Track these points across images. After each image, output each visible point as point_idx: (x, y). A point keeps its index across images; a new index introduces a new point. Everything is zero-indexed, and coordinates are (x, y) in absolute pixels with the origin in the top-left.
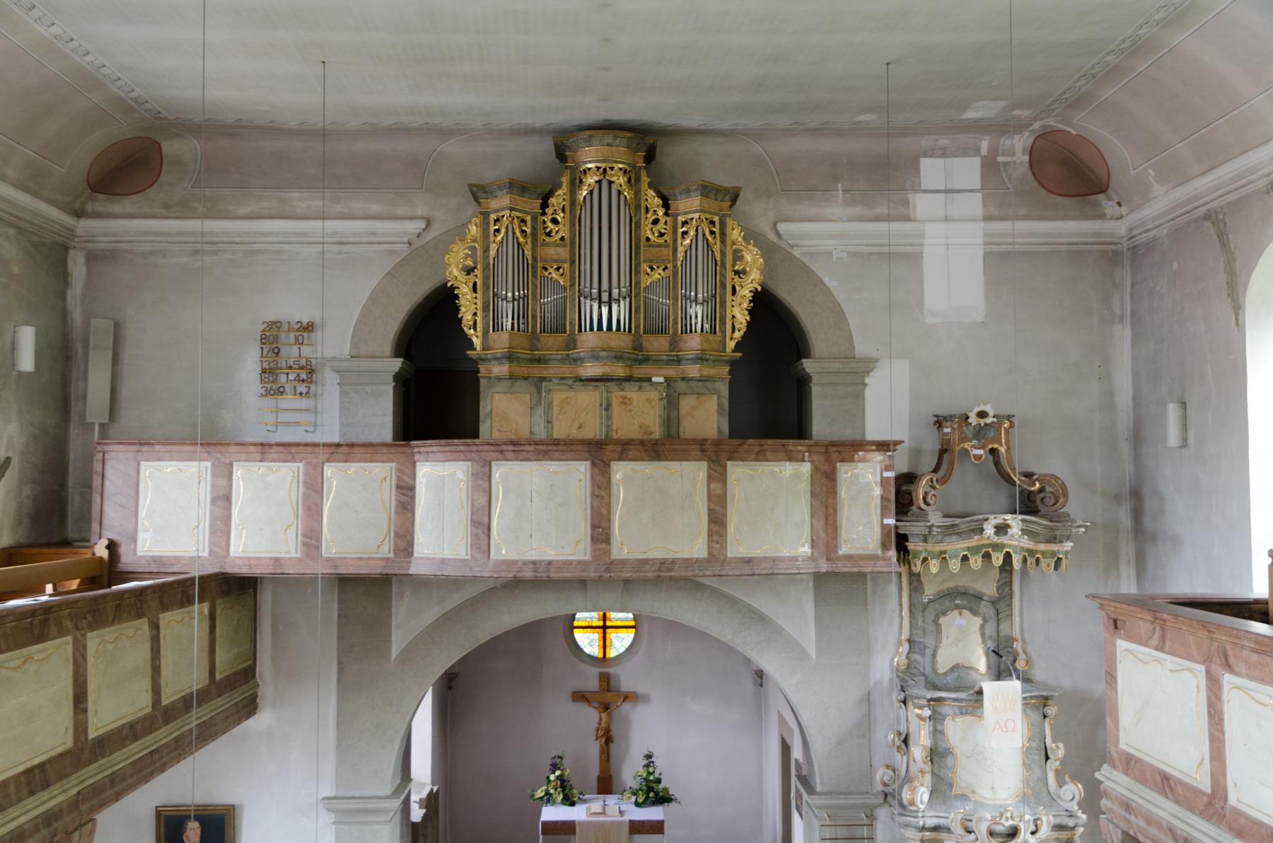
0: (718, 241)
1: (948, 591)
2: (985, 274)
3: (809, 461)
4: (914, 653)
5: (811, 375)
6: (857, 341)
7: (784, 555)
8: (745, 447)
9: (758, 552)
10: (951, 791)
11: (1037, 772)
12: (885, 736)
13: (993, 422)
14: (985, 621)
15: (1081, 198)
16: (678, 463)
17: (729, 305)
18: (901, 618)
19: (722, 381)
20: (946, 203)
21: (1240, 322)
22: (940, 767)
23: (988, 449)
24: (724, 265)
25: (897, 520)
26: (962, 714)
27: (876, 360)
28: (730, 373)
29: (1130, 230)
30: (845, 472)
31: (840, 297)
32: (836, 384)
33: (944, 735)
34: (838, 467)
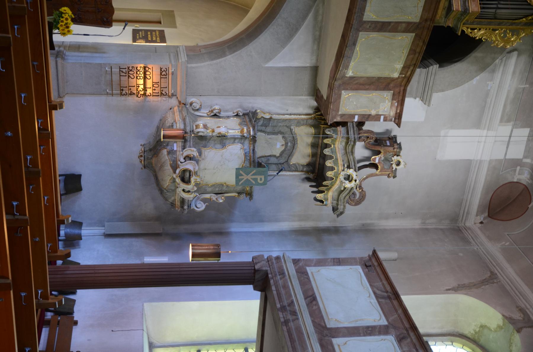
0: (527, 21)
1: (296, 139)
2: (461, 160)
3: (399, 77)
4: (264, 121)
5: (427, 69)
6: (440, 94)
7: (351, 63)
8: (421, 44)
9: (358, 49)
10: (202, 147)
11: (209, 190)
12: (217, 103)
13: (393, 168)
14: (277, 157)
15: (488, 205)
16: (423, 5)
17: (488, 27)
18: (284, 115)
19: (444, 22)
20: (503, 141)
21: (449, 291)
22: (215, 141)
23: (378, 165)
24: (512, 24)
25: (356, 122)
26: (245, 153)
27: (429, 106)
28: (449, 27)
29: (469, 229)
30: (388, 95)
31: (466, 85)
32: (418, 83)
33: (233, 143)
34: (391, 91)
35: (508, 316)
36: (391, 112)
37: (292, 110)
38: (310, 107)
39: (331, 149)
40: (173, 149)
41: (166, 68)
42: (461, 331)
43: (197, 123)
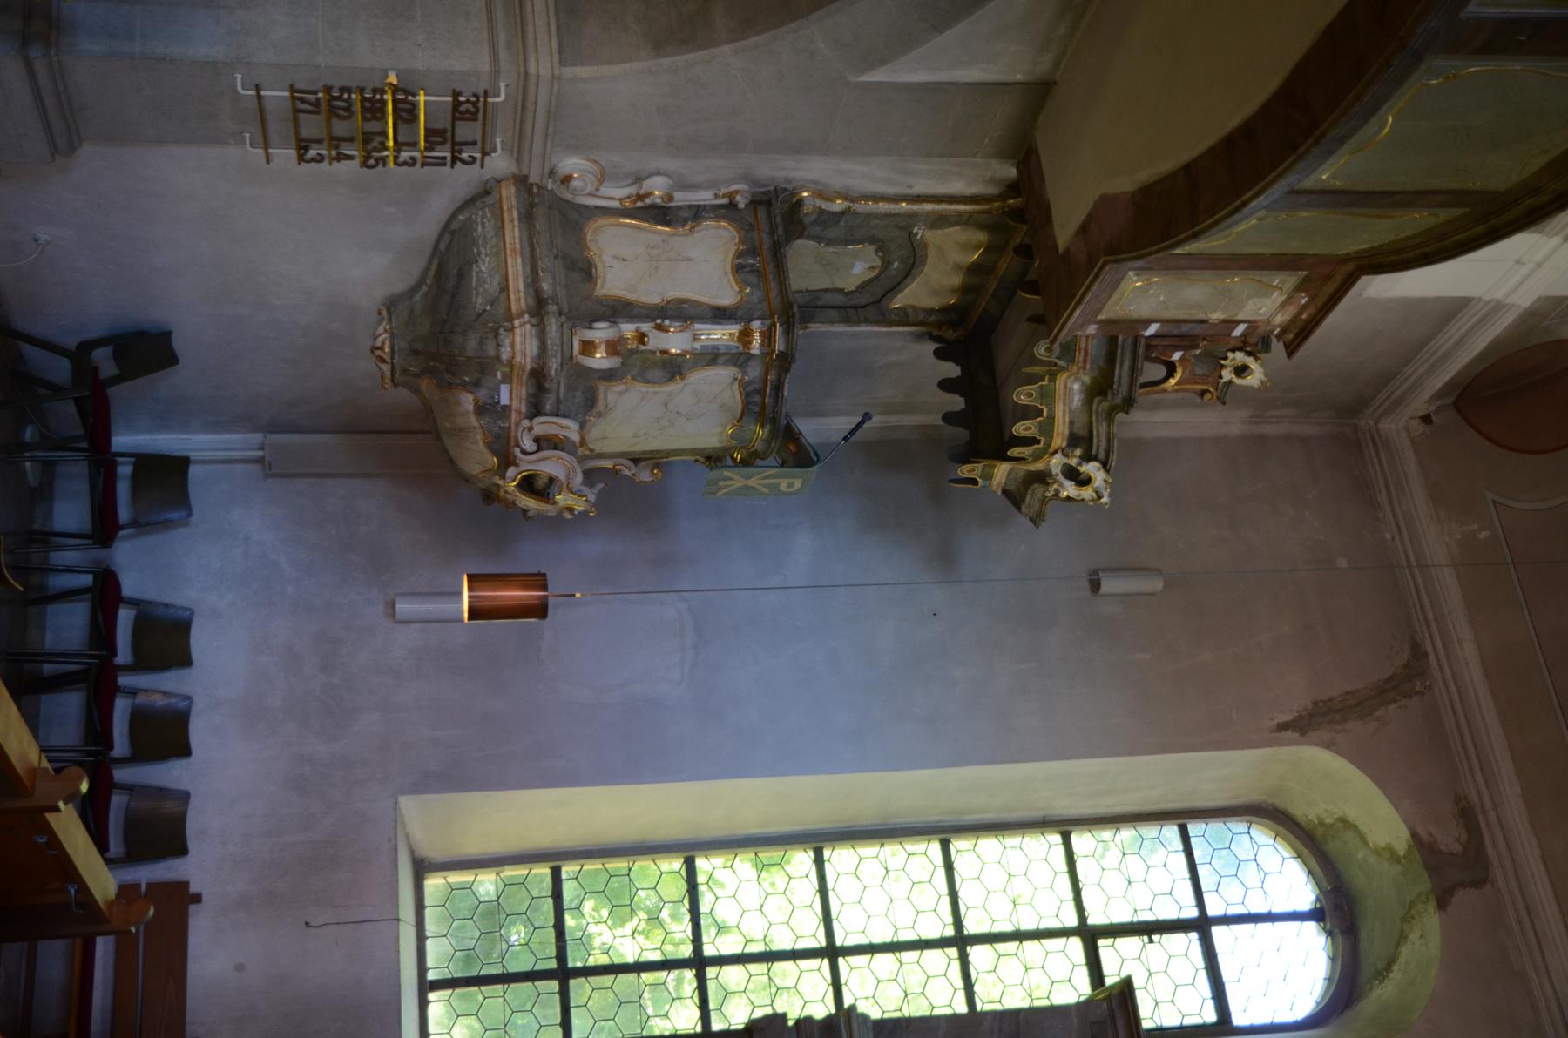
2: (1438, 298)
23: (1177, 364)
26: (748, 395)
35: (1425, 836)
36: (1280, 315)
37: (922, 187)
38: (991, 181)
39: (1042, 385)
40: (496, 400)
41: (475, 95)
42: (1281, 803)
43: (590, 335)
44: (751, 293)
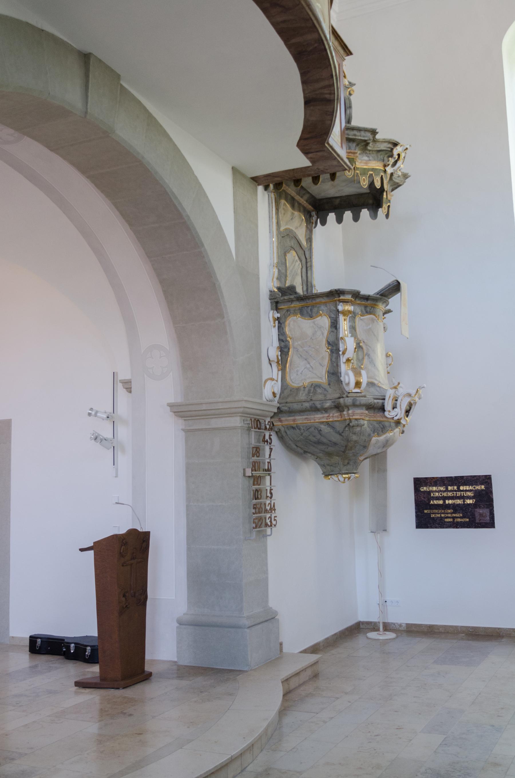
44: (322, 310)
